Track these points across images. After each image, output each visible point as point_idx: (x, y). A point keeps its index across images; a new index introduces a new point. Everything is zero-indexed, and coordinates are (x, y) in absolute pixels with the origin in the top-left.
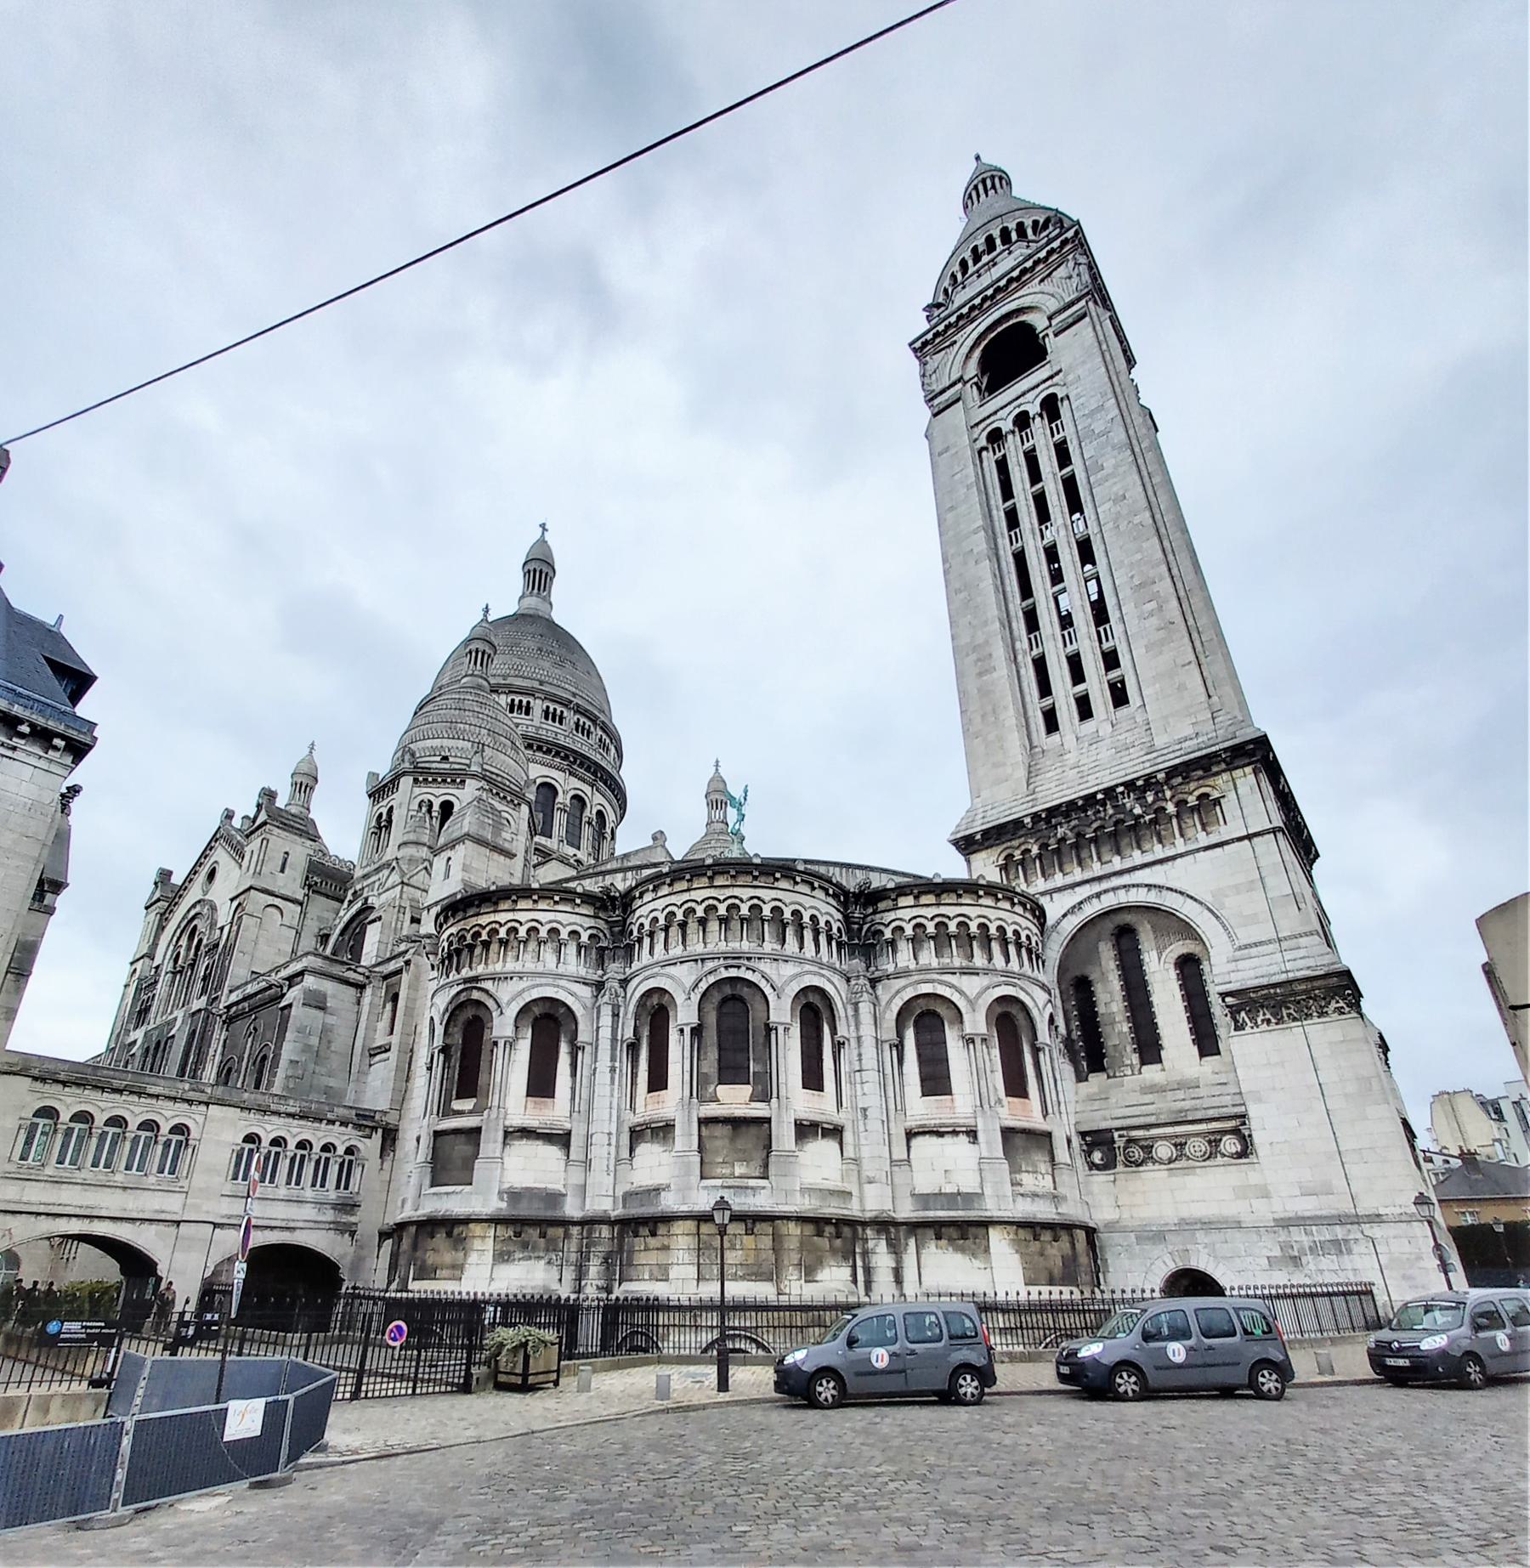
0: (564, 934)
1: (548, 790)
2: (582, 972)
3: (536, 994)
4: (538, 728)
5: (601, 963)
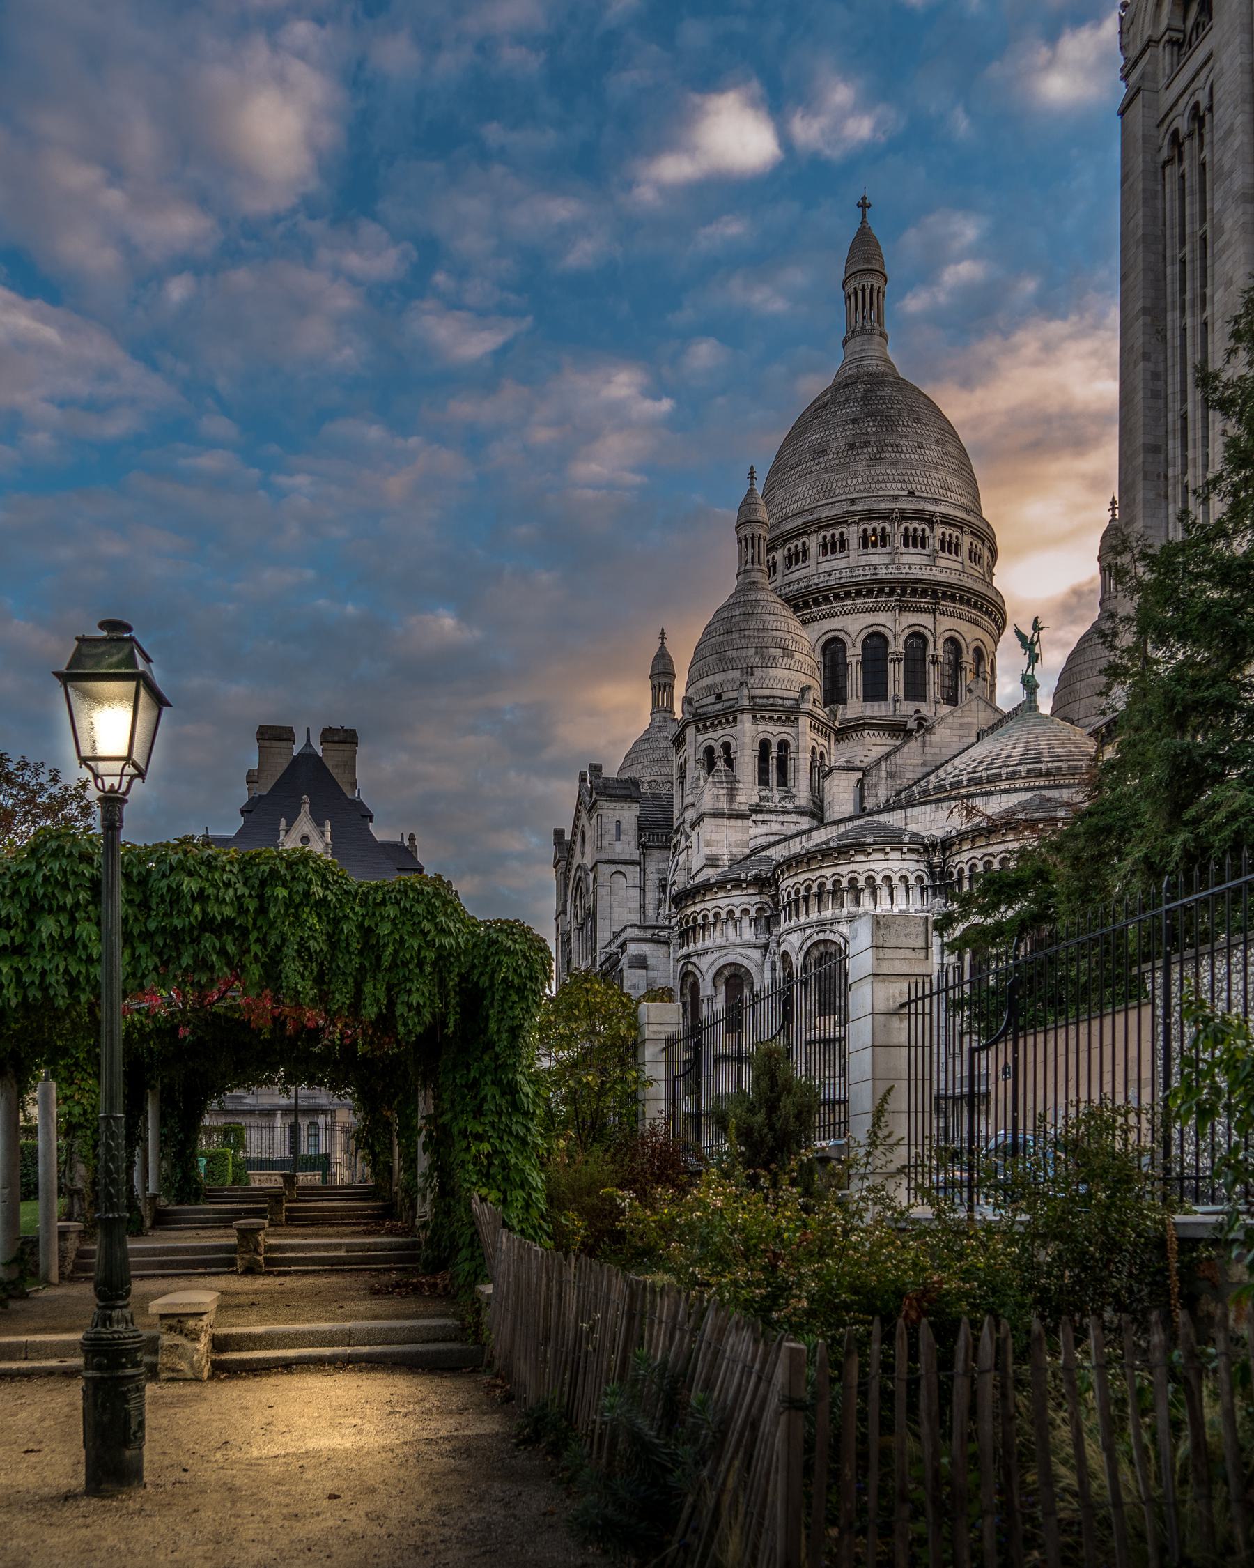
0: (737, 914)
1: (875, 643)
2: (753, 940)
3: (722, 962)
4: (852, 569)
5: (768, 929)
